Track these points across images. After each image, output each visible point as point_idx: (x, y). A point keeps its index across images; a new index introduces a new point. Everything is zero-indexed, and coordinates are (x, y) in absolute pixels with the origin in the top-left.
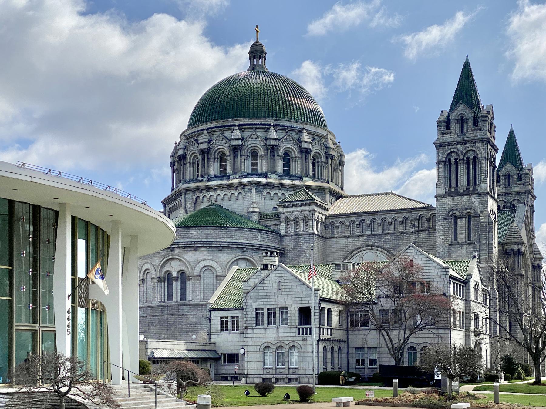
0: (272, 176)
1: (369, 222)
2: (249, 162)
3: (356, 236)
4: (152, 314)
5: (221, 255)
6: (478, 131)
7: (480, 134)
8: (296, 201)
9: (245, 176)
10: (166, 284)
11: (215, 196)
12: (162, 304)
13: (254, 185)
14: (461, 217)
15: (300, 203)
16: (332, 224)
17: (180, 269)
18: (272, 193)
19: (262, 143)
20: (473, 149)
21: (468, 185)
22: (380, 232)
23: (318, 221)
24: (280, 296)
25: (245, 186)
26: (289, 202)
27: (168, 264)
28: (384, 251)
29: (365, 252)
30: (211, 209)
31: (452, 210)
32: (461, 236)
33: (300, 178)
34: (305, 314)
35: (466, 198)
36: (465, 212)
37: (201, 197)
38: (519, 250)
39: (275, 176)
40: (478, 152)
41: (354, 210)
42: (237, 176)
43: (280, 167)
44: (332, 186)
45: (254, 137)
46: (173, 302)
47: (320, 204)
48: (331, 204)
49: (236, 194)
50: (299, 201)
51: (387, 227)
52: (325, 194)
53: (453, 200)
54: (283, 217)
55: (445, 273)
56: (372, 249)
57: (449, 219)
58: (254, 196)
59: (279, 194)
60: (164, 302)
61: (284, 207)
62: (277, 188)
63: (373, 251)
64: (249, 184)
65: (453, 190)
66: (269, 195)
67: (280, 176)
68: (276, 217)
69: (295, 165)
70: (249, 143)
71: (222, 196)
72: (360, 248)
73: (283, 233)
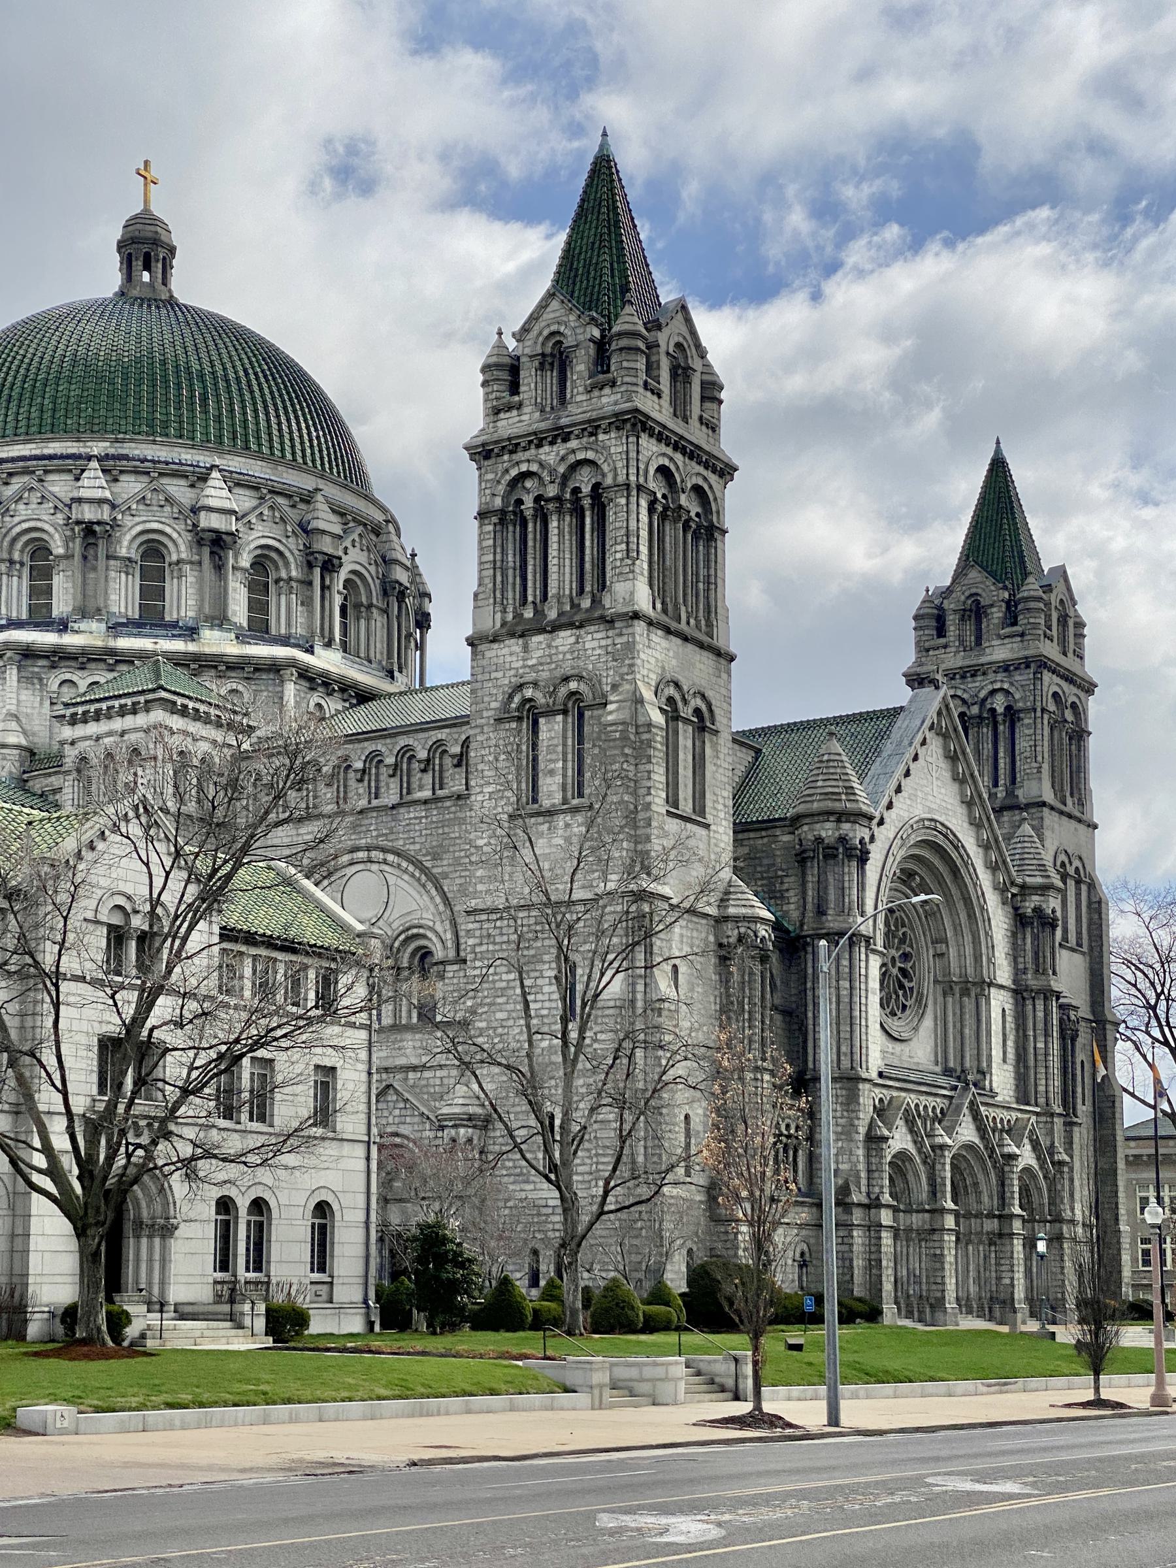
0: (83, 626)
1: (359, 765)
6: (607, 391)
7: (613, 398)
13: (9, 654)
14: (550, 713)
15: (116, 703)
18: (83, 681)
19: (60, 518)
20: (590, 455)
21: (581, 591)
22: (391, 796)
28: (404, 864)
31: (520, 687)
32: (549, 780)
33: (191, 632)
35: (565, 638)
36: (563, 691)
38: (843, 840)
40: (605, 468)
43: (122, 594)
45: (35, 497)
50: (120, 696)
51: (415, 781)
53: (526, 649)
57: (511, 719)
61: (73, 721)
62: (102, 665)
63: (375, 867)
65: (529, 614)
69: (179, 591)
70: (16, 519)
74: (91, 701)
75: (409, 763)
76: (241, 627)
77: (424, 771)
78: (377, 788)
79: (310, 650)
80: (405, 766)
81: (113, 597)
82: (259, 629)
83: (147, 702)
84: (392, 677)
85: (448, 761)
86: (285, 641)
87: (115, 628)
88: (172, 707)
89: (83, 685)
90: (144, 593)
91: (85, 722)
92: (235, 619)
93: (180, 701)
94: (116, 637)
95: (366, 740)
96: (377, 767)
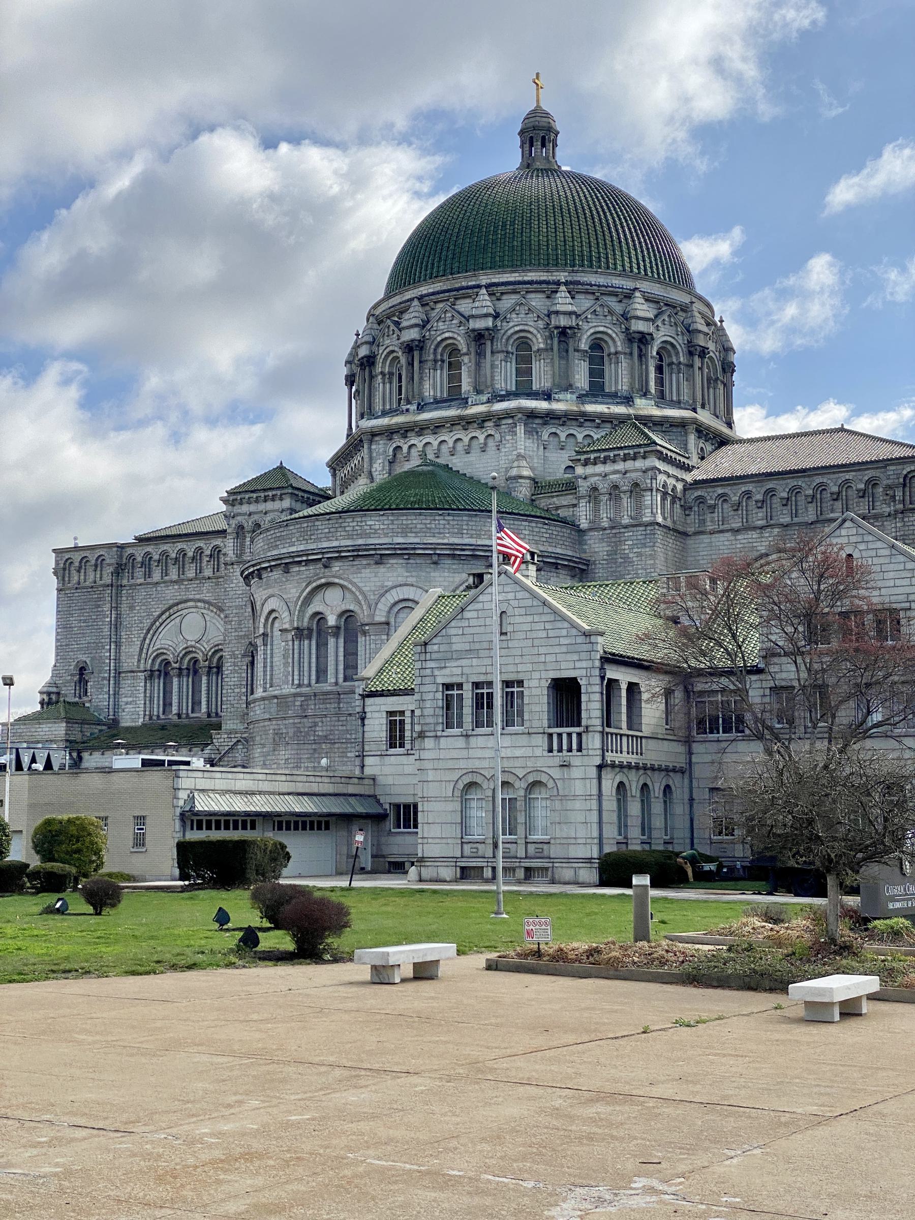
0: (561, 396)
1: (785, 495)
2: (511, 367)
3: (755, 528)
4: (281, 715)
5: (437, 574)
8: (614, 449)
9: (503, 398)
10: (314, 643)
11: (435, 444)
12: (304, 690)
13: (520, 415)
15: (621, 453)
16: (701, 500)
17: (344, 608)
23: (665, 494)
26: (599, 451)
27: (318, 597)
30: (421, 474)
33: (628, 400)
34: (566, 693)
37: (405, 448)
39: (569, 396)
41: (753, 470)
42: (484, 398)
44: (704, 417)
46: (326, 687)
47: (674, 456)
48: (702, 458)
49: (482, 438)
50: (621, 448)
51: (827, 505)
52: (686, 434)
54: (583, 487)
58: (521, 441)
59: (580, 437)
60: (309, 685)
61: (586, 463)
62: (574, 423)
64: (508, 414)
66: (556, 439)
67: (580, 397)
68: (570, 487)
71: (451, 445)
72: (767, 555)
73: (584, 524)
77: (836, 500)
79: (694, 410)
80: (818, 496)
81: (577, 377)
82: (662, 398)
85: (852, 493)
86: (678, 404)
89: (563, 438)
90: (592, 373)
91: (595, 464)
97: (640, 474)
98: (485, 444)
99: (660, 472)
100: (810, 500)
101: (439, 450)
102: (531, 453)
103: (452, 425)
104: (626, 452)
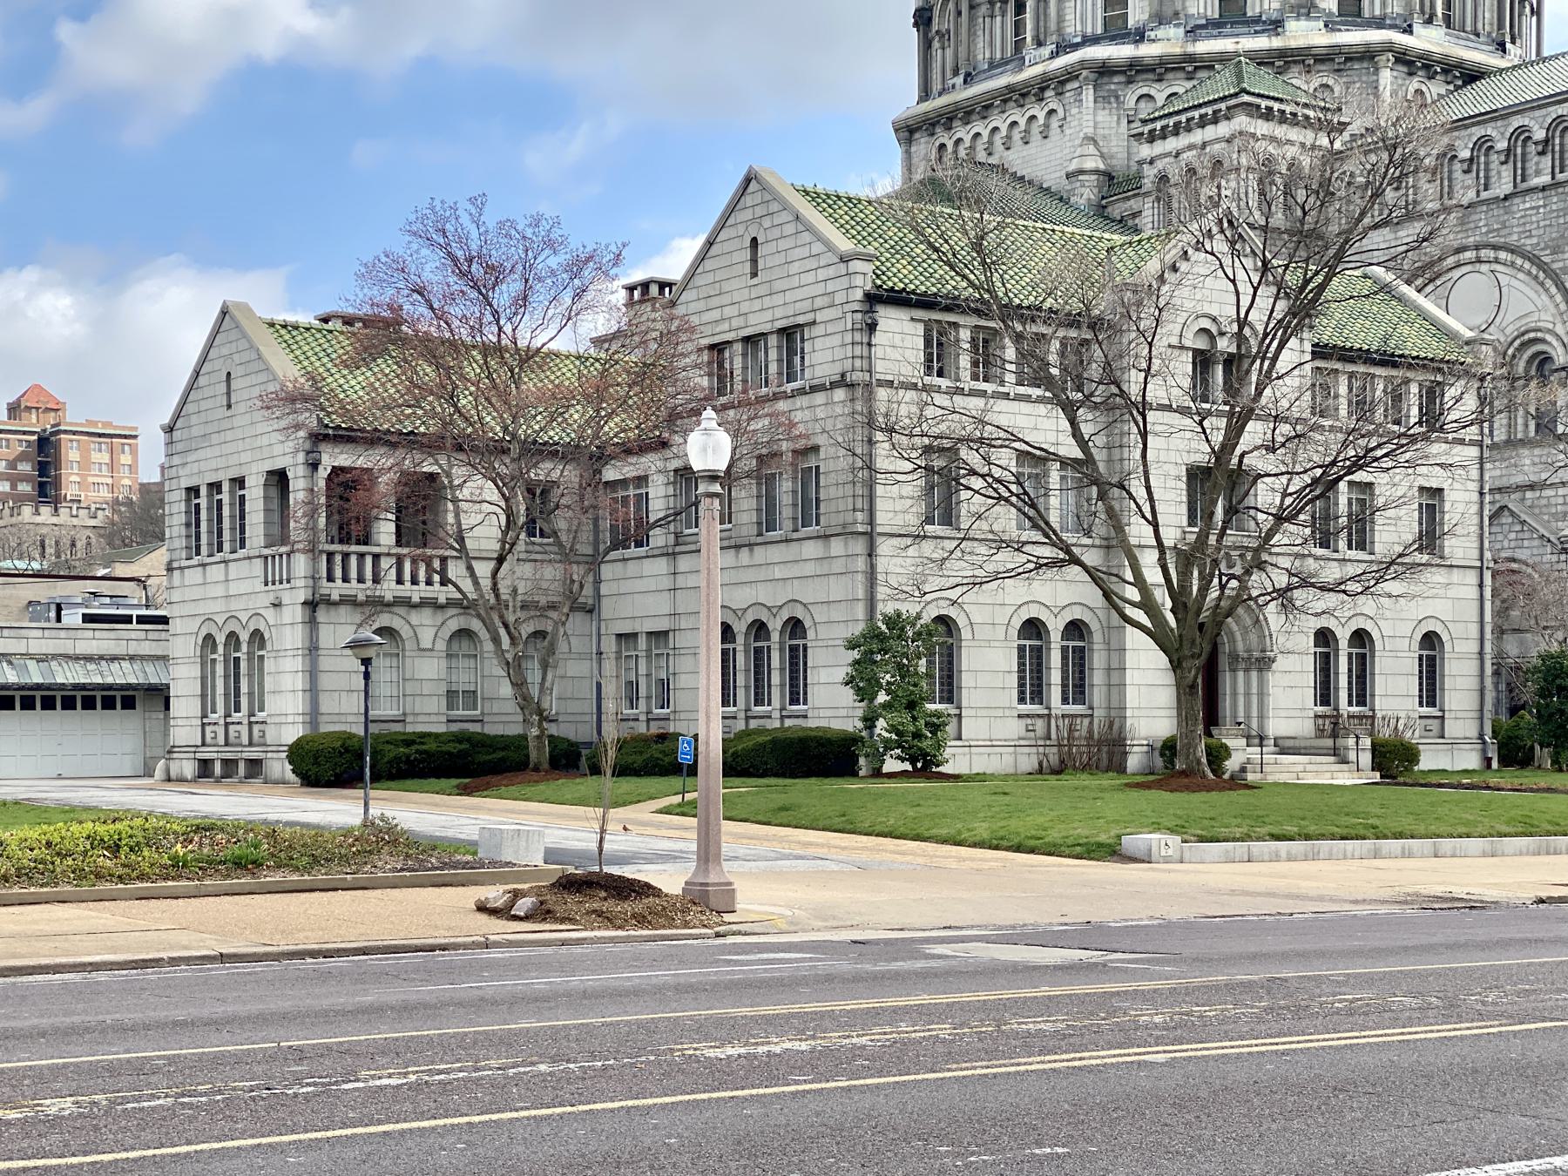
1: (1466, 154)
11: (985, 134)
13: (1085, 73)
15: (1196, 114)
18: (1160, 93)
22: (1503, 186)
24: (229, 435)
25: (1062, 83)
28: (1519, 261)
29: (1456, 274)
33: (1276, 26)
42: (1046, 51)
49: (1041, 116)
50: (1200, 106)
54: (1150, 173)
55: (844, 282)
56: (1479, 261)
61: (1152, 138)
62: (1181, 75)
63: (1484, 268)
64: (1070, 75)
71: (1004, 132)
74: (1170, 115)
75: (1524, 146)
76: (1331, 14)
77: (1542, 153)
78: (1487, 178)
79: (1408, 30)
80: (1519, 150)
83: (1228, 108)
84: (1504, 51)
86: (1379, 23)
87: (1193, 32)
88: (1252, 110)
89: (1160, 98)
91: (1164, 138)
92: (1322, 5)
93: (1264, 103)
94: (1195, 41)
95: (1473, 125)
96: (1486, 155)
97: (1224, 145)
98: (1047, 126)
99: (1253, 135)
100: (1503, 158)
101: (991, 142)
102: (1107, 132)
103: (1005, 101)
104: (1203, 111)
